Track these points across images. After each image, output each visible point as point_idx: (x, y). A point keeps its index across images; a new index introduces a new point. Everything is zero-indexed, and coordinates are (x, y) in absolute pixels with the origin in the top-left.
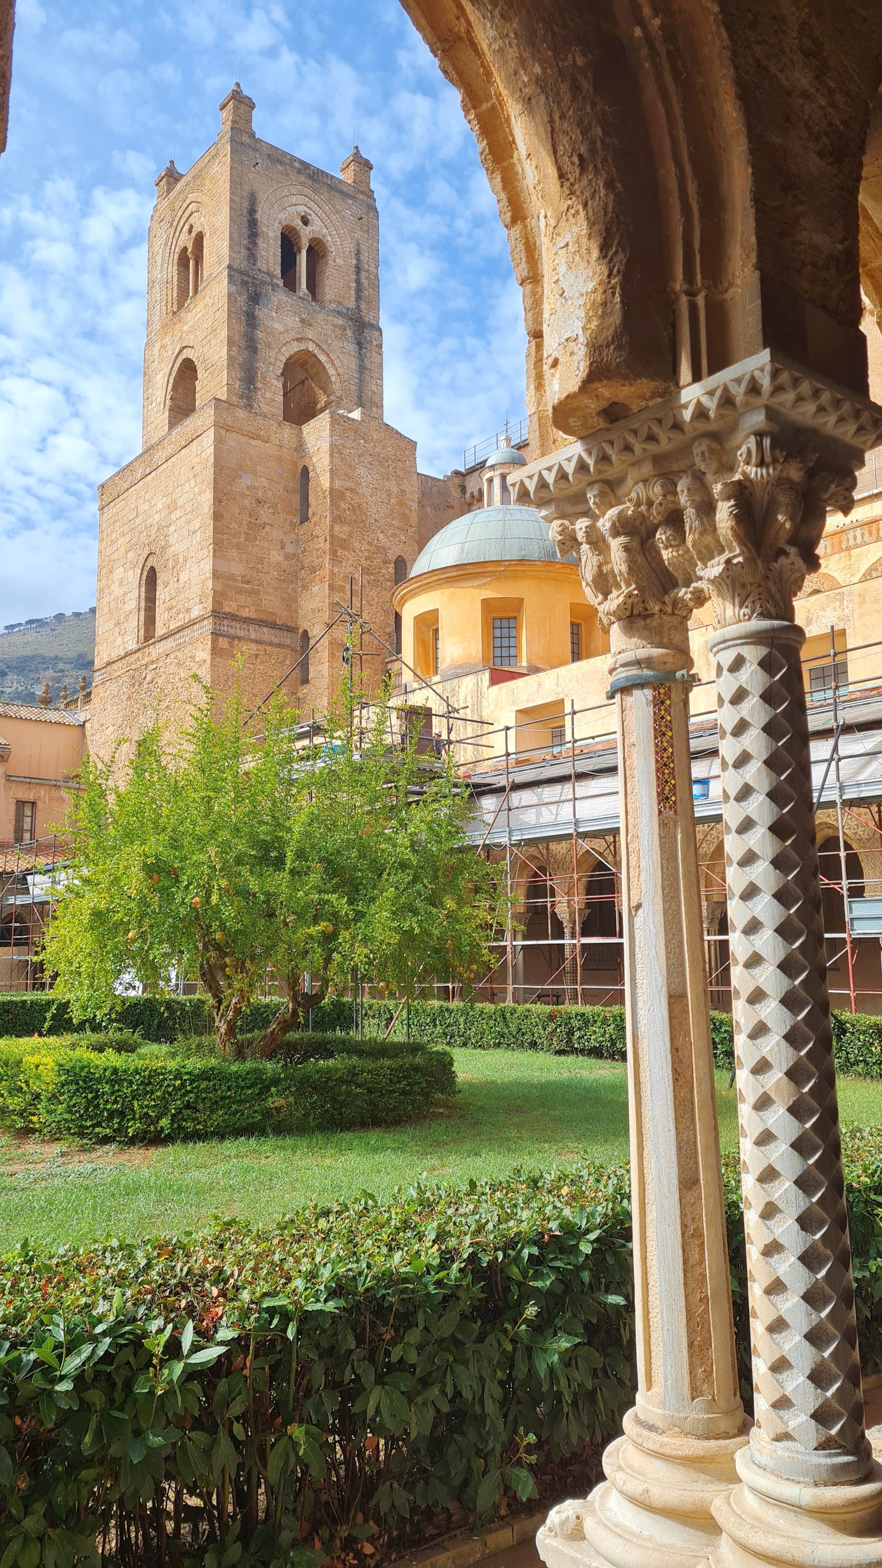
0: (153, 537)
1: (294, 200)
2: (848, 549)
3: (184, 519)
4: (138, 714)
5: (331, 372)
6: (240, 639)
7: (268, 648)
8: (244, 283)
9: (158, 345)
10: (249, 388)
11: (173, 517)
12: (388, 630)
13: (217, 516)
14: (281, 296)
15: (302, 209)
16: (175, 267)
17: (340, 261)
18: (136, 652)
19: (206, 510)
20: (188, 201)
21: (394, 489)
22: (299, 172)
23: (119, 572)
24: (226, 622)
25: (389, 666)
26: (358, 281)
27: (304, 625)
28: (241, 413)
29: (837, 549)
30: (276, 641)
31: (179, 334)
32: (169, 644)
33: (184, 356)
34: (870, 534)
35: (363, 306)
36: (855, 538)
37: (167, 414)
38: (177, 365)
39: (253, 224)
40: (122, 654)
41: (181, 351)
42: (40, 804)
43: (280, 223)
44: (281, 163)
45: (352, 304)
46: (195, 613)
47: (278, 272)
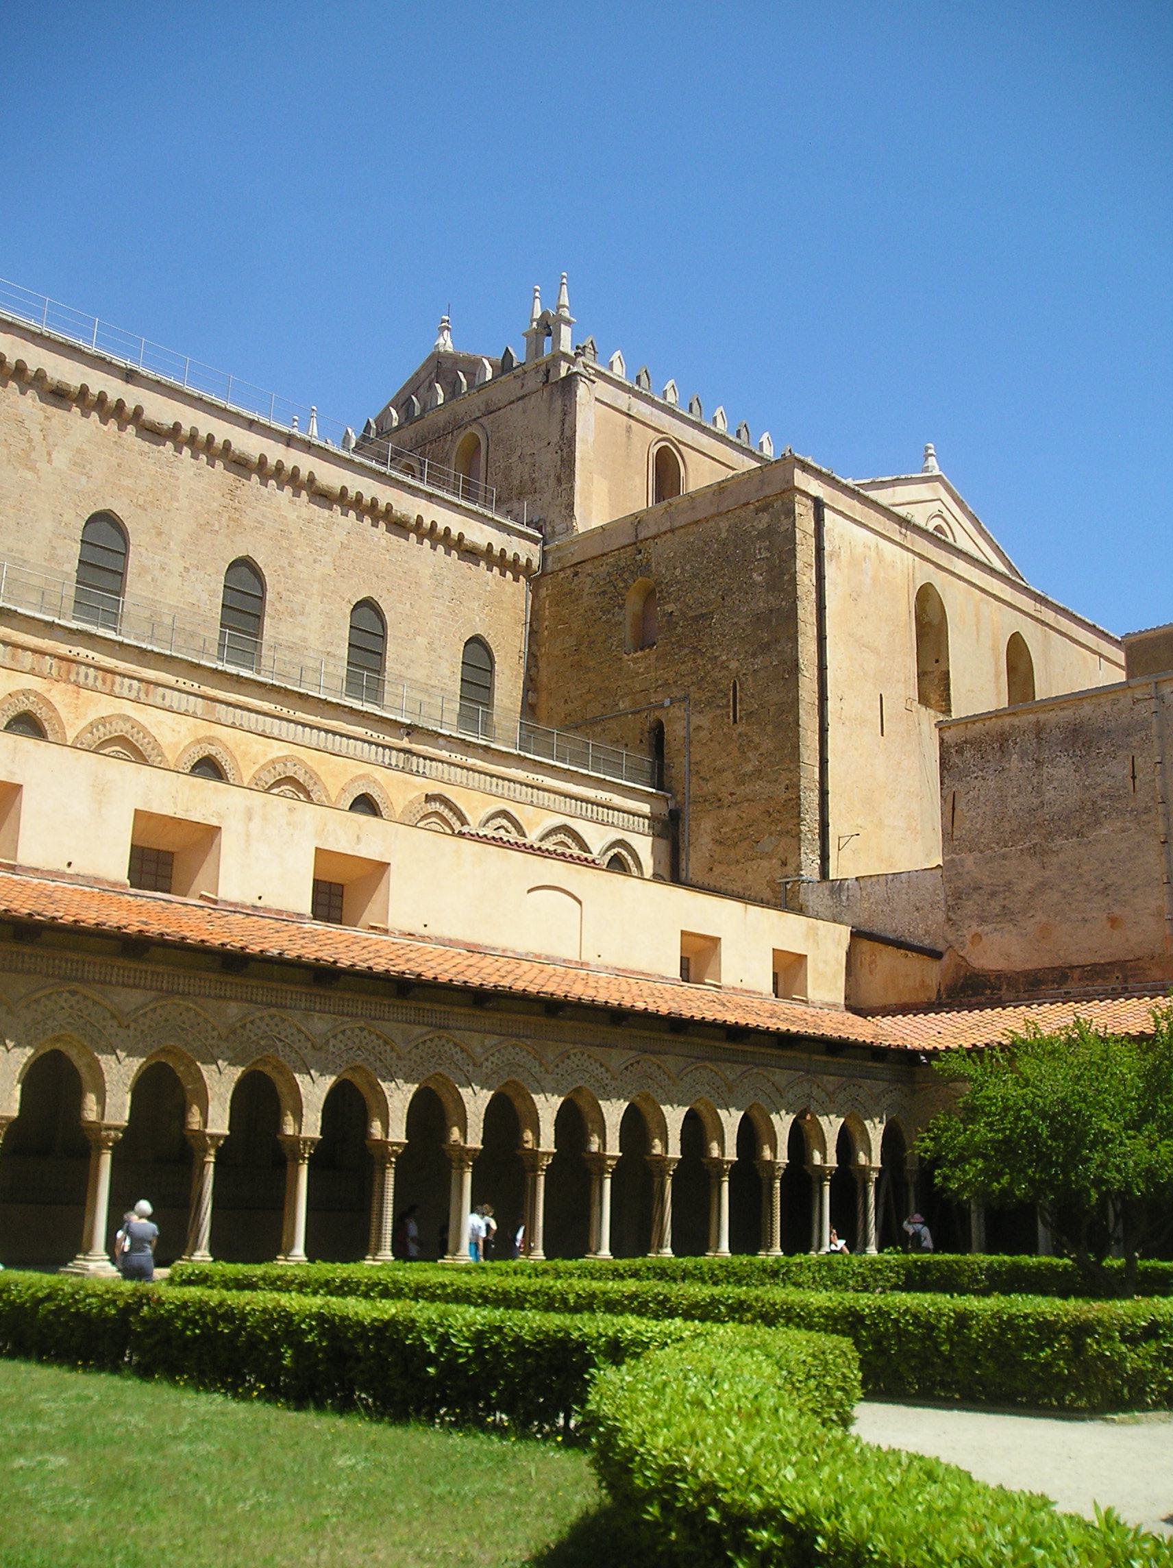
36: (87, 676)
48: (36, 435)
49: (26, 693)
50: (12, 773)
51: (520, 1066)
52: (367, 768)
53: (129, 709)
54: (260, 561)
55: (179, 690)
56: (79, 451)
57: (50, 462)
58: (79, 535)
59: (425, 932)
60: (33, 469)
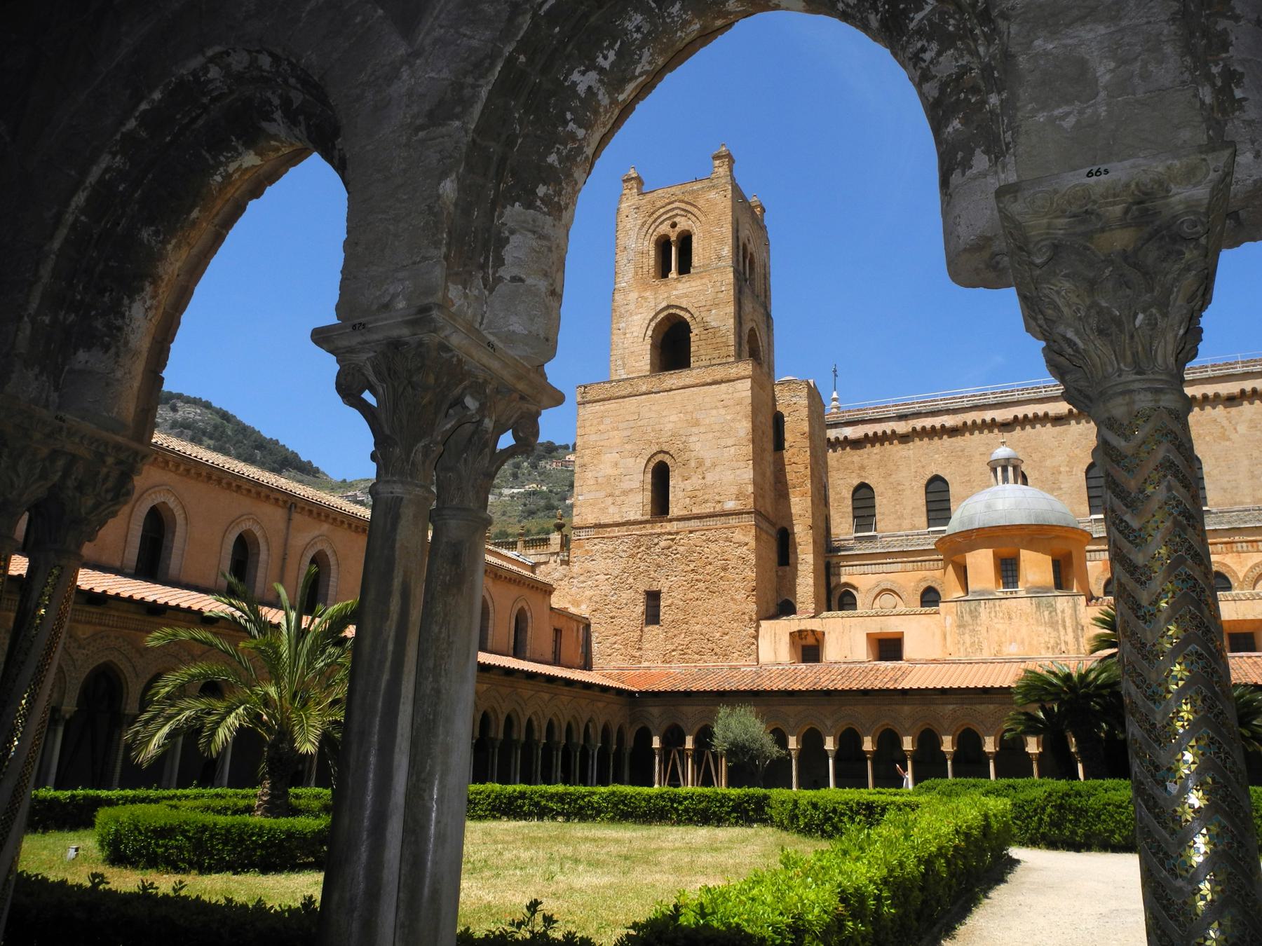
3: (711, 435)
11: (695, 430)
13: (753, 442)
16: (652, 246)
31: (666, 295)
32: (694, 524)
39: (738, 238)
41: (669, 307)
45: (762, 298)
46: (730, 505)
48: (1225, 423)
56: (1251, 420)
57: (1237, 432)
60: (1229, 439)
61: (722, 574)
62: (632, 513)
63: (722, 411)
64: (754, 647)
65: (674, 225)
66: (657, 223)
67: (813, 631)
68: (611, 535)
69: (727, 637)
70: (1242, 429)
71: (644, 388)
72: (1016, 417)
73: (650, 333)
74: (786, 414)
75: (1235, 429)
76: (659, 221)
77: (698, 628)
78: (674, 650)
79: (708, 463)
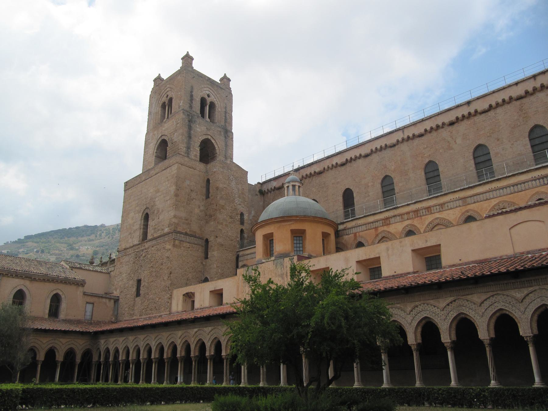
0: (148, 202)
1: (205, 89)
2: (421, 216)
4: (138, 269)
5: (216, 146)
6: (183, 241)
7: (193, 245)
8: (188, 115)
9: (151, 134)
10: (188, 150)
11: (158, 195)
12: (238, 239)
13: (176, 195)
14: (200, 120)
15: (208, 92)
17: (220, 110)
18: (138, 245)
19: (172, 193)
20: (167, 87)
21: (240, 188)
22: (207, 80)
23: (132, 214)
24: (178, 235)
25: (238, 253)
26: (225, 116)
27: (207, 237)
28: (186, 159)
29: (416, 216)
30: (196, 242)
31: (161, 131)
32: (154, 242)
33: (163, 137)
34: (428, 211)
35: (227, 125)
36: (423, 213)
37: (154, 157)
38: (159, 141)
39: (192, 96)
40: (132, 245)
41: (162, 136)
42: (95, 304)
43: (200, 96)
44: (202, 77)
45: (223, 123)
46: (166, 230)
47: (199, 112)
49: (407, 226)
50: (326, 265)
51: (396, 314)
52: (537, 190)
53: (437, 215)
54: (541, 123)
55: (452, 201)
56: (463, 135)
57: (456, 143)
58: (472, 157)
59: (461, 262)
61: (161, 267)
62: (136, 241)
63: (167, 183)
64: (169, 304)
65: (168, 96)
66: (161, 98)
67: (191, 293)
68: (129, 253)
69: (160, 300)
70: (459, 141)
71: (143, 178)
72: (347, 160)
73: (155, 151)
74: (210, 179)
75: (455, 142)
76: (162, 96)
77: (151, 296)
78: (143, 309)
79: (160, 211)
